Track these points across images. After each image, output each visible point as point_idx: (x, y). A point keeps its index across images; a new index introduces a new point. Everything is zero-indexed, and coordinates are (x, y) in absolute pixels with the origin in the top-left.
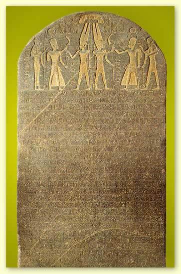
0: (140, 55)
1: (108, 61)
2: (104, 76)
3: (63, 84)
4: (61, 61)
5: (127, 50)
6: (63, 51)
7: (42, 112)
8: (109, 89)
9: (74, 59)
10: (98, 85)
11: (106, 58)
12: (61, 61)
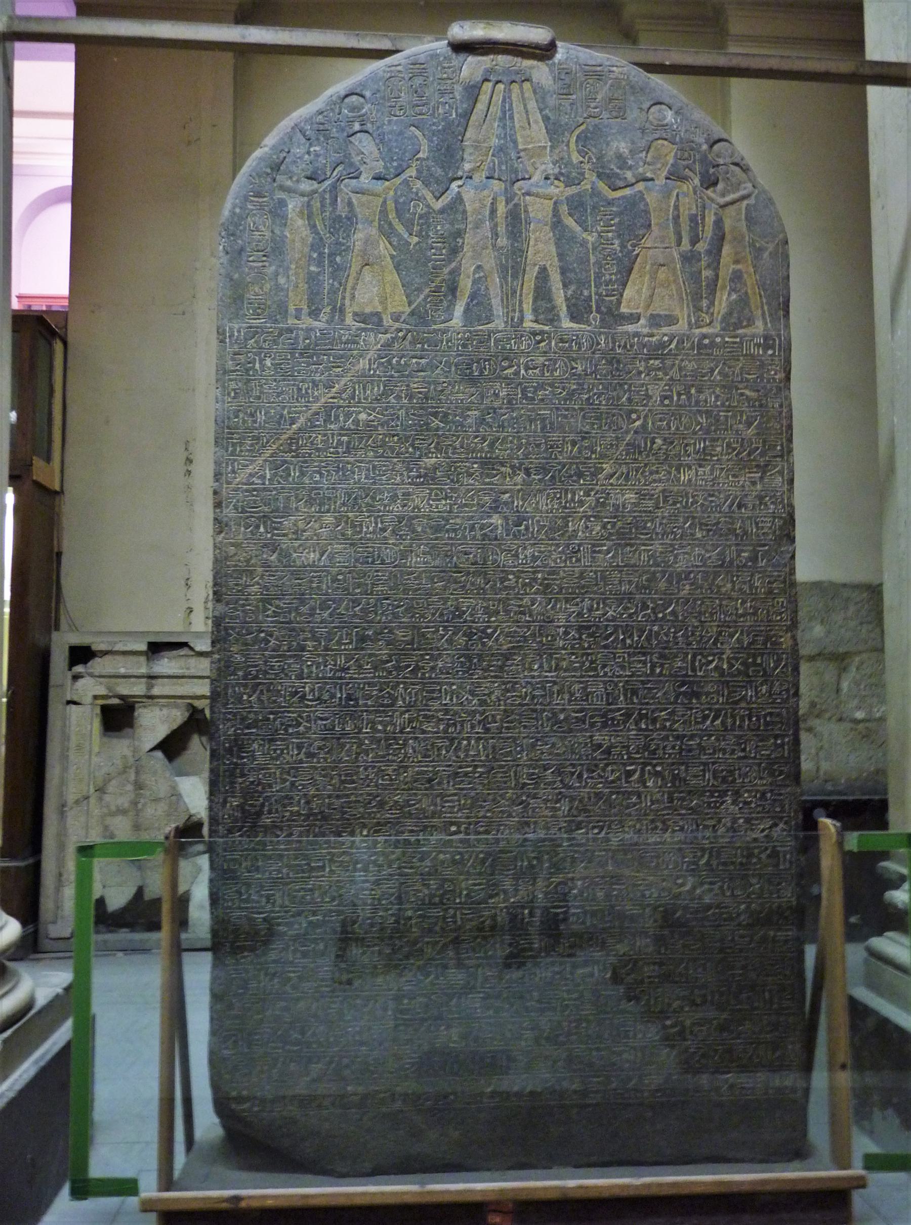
0: (688, 207)
1: (570, 222)
2: (555, 278)
3: (399, 303)
4: (392, 216)
5: (641, 186)
6: (403, 176)
7: (315, 407)
8: (572, 325)
9: (442, 211)
10: (535, 310)
11: (564, 209)
12: (392, 216)
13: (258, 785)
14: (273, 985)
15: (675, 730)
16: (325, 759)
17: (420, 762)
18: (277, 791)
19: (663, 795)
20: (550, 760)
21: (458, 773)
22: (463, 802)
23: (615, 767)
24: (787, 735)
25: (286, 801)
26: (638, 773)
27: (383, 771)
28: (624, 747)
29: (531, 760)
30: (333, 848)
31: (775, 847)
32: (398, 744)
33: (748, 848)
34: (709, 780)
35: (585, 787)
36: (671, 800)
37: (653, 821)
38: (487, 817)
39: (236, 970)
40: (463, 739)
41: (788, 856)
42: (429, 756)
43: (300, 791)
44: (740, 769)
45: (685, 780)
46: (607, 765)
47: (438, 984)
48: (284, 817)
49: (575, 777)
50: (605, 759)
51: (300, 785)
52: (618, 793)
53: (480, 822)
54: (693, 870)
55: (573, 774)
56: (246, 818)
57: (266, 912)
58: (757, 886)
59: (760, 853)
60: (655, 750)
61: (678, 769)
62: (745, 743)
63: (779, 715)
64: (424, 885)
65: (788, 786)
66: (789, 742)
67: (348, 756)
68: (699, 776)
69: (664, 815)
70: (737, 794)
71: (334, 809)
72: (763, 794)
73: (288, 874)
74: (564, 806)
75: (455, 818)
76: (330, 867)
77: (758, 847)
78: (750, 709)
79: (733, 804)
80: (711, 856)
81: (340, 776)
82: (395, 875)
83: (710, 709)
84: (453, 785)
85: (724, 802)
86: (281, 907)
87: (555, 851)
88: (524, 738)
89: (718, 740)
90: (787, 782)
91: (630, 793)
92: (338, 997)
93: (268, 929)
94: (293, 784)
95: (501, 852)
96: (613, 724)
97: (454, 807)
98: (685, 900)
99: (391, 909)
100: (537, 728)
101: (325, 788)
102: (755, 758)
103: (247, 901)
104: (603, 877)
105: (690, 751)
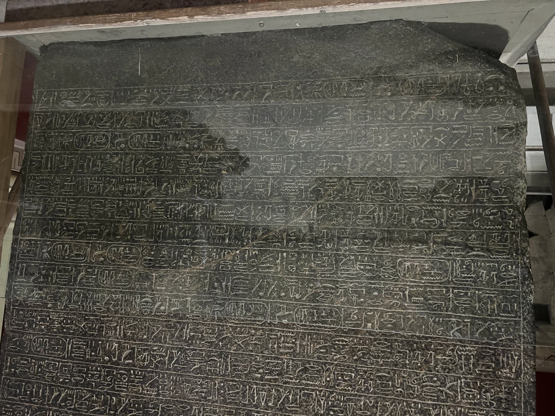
13: (481, 388)
14: (463, 186)
15: (89, 391)
16: (409, 406)
17: (313, 390)
18: (460, 378)
19: (107, 333)
20: (196, 377)
21: (278, 375)
22: (276, 346)
23: (141, 363)
24: (7, 374)
25: (450, 366)
26: (124, 356)
27: (351, 386)
28: (133, 381)
29: (212, 379)
30: (402, 313)
31: (28, 282)
32: (334, 411)
33: (47, 283)
34: (69, 344)
35: (168, 348)
36: (100, 329)
37: (116, 312)
38: (254, 329)
39: (502, 202)
40: (272, 408)
41: (19, 273)
42: (304, 395)
43: (436, 376)
44: (45, 350)
45: (87, 345)
46: (147, 366)
47: (306, 183)
48: (453, 350)
49: (175, 359)
50: (149, 372)
51: (435, 382)
52: (141, 340)
53: (262, 325)
54: (90, 267)
55: (177, 362)
56: (493, 354)
57: (469, 256)
58: (44, 251)
59: (39, 277)
60: (107, 376)
61: (91, 355)
62: (38, 372)
63: (10, 394)
64: (314, 271)
65: (12, 331)
66: (6, 369)
67: (385, 406)
68: (76, 348)
69: (108, 316)
70: (49, 329)
71: (399, 352)
72: (30, 326)
73: (448, 292)
74: (187, 333)
75: (283, 331)
76: (404, 295)
77: (40, 283)
78: (31, 402)
79: (54, 320)
80: (75, 280)
81: (393, 386)
82: (341, 282)
83: (60, 407)
84: (284, 363)
85: (60, 323)
86: (455, 260)
87: (198, 293)
88: (216, 401)
89: (58, 378)
90: (11, 334)
91: (133, 339)
92: (398, 174)
93: (468, 240)
94: (443, 384)
95: (244, 296)
96: (139, 405)
97: (283, 342)
98: (100, 243)
99: (346, 251)
100: (204, 409)
101: (410, 375)
102: (32, 358)
103: (493, 269)
104: (161, 267)
105: (80, 371)
